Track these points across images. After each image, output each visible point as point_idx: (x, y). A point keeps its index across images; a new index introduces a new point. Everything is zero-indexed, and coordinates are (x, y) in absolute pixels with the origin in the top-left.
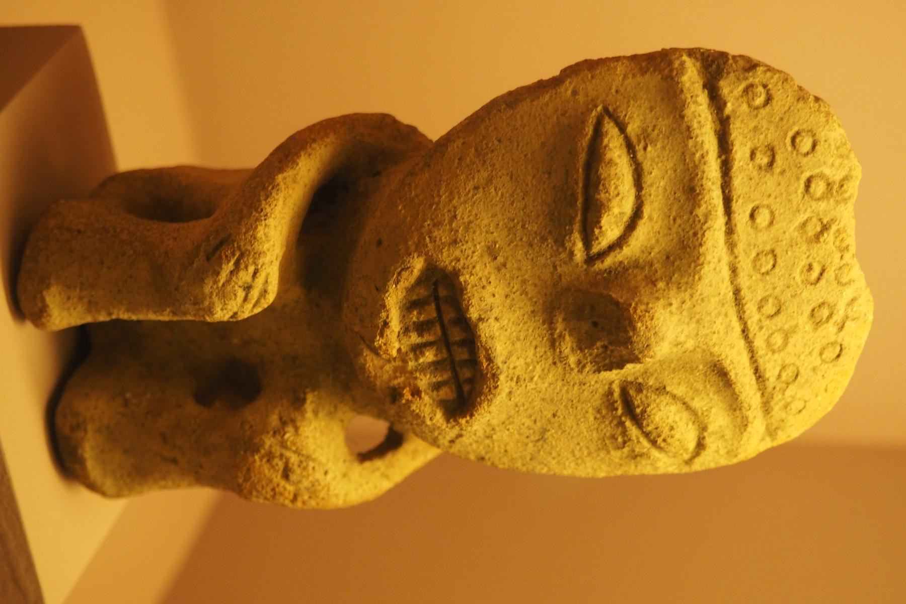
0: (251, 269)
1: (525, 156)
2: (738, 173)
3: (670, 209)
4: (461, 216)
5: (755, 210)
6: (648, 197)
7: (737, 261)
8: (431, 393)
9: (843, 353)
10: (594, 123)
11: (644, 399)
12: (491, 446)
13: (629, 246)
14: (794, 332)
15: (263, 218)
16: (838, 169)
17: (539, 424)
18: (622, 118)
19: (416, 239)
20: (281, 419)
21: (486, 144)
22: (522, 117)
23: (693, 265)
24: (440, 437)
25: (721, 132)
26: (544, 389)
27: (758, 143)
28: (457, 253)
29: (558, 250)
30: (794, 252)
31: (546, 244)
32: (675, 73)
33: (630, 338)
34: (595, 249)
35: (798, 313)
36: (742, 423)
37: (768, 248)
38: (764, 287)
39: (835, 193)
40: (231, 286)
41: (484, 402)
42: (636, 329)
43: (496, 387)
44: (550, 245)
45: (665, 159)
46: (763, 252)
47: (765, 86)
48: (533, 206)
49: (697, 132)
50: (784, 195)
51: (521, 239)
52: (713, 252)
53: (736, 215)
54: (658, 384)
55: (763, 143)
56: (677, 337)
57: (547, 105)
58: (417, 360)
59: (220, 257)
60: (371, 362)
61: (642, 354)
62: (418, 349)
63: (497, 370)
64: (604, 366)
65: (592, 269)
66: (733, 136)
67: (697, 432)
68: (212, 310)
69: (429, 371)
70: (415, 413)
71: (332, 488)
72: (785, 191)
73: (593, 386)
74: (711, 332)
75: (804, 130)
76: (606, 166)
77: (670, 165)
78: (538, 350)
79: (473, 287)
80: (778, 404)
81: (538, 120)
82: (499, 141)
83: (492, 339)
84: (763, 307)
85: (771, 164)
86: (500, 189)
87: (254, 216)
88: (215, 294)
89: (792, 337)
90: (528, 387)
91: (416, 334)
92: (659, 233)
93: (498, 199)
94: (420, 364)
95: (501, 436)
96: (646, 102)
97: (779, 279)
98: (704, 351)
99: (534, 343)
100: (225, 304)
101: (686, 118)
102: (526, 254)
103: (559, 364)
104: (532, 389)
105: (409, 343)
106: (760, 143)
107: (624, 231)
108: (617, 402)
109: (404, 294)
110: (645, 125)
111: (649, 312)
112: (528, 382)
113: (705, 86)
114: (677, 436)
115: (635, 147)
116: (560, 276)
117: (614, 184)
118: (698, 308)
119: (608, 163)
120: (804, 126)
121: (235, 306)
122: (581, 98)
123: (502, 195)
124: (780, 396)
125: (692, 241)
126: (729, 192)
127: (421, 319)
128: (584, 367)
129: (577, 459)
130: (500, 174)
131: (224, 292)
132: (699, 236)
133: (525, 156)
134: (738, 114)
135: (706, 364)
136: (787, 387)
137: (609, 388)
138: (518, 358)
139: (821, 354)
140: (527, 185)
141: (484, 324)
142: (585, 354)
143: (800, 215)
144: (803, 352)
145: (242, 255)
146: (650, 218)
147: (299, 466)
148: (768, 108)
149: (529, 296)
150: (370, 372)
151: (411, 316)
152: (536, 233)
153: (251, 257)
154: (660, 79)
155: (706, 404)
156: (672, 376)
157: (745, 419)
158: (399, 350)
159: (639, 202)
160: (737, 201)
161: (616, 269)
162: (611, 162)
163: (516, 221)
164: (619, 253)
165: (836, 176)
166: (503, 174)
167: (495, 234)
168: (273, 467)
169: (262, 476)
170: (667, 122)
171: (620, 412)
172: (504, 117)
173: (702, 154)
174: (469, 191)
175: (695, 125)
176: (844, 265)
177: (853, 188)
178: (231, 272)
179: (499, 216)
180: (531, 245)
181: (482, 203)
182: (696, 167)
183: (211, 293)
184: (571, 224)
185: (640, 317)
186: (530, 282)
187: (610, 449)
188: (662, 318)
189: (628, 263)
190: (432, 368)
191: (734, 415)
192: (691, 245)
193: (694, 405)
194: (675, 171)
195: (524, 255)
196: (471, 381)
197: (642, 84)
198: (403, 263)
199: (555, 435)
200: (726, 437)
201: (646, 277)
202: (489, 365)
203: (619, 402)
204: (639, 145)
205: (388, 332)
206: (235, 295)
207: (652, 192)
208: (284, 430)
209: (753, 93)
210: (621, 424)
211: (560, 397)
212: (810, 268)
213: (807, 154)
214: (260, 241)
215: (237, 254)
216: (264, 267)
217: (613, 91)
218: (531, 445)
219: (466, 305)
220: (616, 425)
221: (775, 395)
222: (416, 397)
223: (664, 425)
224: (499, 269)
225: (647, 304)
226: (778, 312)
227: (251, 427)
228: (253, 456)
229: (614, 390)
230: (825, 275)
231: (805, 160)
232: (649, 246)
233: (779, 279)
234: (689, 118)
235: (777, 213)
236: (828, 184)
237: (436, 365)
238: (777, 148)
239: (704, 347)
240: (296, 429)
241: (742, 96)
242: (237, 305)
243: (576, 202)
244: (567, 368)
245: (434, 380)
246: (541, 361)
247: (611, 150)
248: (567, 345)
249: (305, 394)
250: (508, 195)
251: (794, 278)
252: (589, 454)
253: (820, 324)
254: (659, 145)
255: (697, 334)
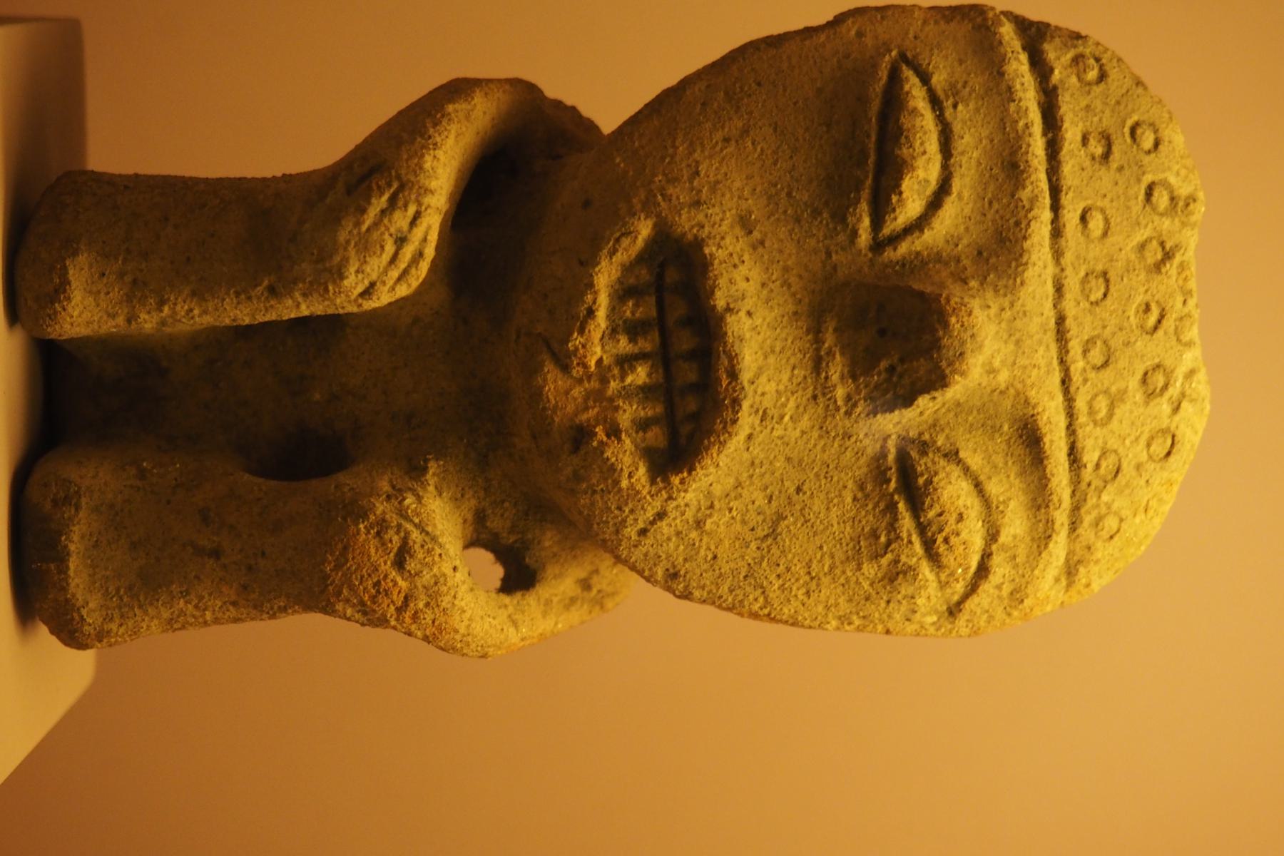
0: (412, 209)
1: (795, 104)
2: (1068, 158)
3: (985, 189)
4: (706, 173)
5: (1087, 212)
6: (958, 168)
7: (1064, 275)
8: (634, 435)
9: (1174, 451)
10: (888, 67)
11: (929, 464)
12: (697, 544)
13: (933, 229)
14: (1122, 400)
15: (431, 146)
16: (1184, 181)
17: (774, 504)
18: (924, 67)
19: (643, 197)
20: (393, 487)
21: (742, 88)
22: (789, 58)
23: (1014, 264)
24: (630, 521)
25: (1046, 105)
26: (793, 440)
27: (1091, 126)
28: (701, 217)
29: (835, 229)
30: (1131, 280)
31: (819, 219)
32: (990, 23)
33: (939, 339)
34: (887, 231)
35: (1128, 371)
36: (1045, 532)
37: (1100, 268)
38: (1093, 323)
39: (1179, 213)
40: (379, 233)
41: (714, 445)
42: (949, 326)
43: (734, 421)
44: (824, 222)
45: (980, 123)
46: (1092, 273)
47: (1098, 60)
48: (805, 169)
49: (1020, 94)
50: (1122, 199)
51: (785, 212)
52: (1039, 251)
53: (1065, 211)
54: (948, 445)
55: (1096, 129)
56: (993, 357)
57: (823, 45)
58: (623, 379)
59: (370, 188)
60: (553, 382)
61: (950, 369)
62: (626, 363)
63: (741, 393)
64: (883, 405)
65: (880, 260)
66: (1062, 111)
67: (984, 542)
68: (343, 271)
69: (636, 399)
70: (609, 463)
71: (459, 595)
72: (1123, 194)
73: (861, 441)
74: (1031, 364)
75: (1144, 121)
76: (910, 115)
77: (985, 133)
78: (796, 372)
79: (721, 263)
80: (1090, 513)
81: (811, 62)
82: (759, 84)
83: (741, 341)
84: (1089, 351)
85: (1106, 156)
86: (759, 143)
87: (420, 143)
88: (353, 244)
89: (1119, 407)
90: (775, 431)
91: (626, 338)
92: (970, 219)
93: (756, 156)
94: (624, 388)
95: (717, 523)
96: (954, 54)
97: (1111, 315)
98: (1018, 394)
99: (792, 361)
100: (365, 262)
101: (1006, 76)
102: (791, 232)
103: (821, 399)
104: (778, 438)
105: (614, 351)
106: (1094, 127)
107: (926, 210)
108: (891, 469)
109: (619, 274)
110: (954, 79)
111: (965, 306)
112: (777, 423)
113: (1024, 49)
114: (964, 535)
115: (942, 102)
116: (835, 268)
117: (920, 138)
118: (1018, 323)
119: (912, 112)
120: (1145, 117)
121: (376, 268)
122: (869, 41)
123: (762, 150)
124: (1094, 500)
125: (1014, 233)
126: (1057, 180)
127: (638, 315)
128: (855, 405)
129: (812, 578)
130: (760, 124)
131: (367, 241)
132: (1023, 226)
133: (795, 104)
134: (1066, 85)
135: (1013, 421)
136: (1105, 487)
137: (882, 447)
138: (769, 381)
139: (1148, 445)
140: (797, 140)
141: (733, 317)
142: (860, 385)
143: (1140, 229)
144: (1129, 435)
145: (402, 187)
146: (960, 197)
147: (422, 546)
148: (1102, 86)
149: (793, 289)
150: (549, 401)
151: (624, 308)
152: (805, 204)
153: (414, 191)
154: (970, 28)
155: (1003, 492)
156: (968, 436)
157: (1050, 524)
158: (600, 361)
159: (947, 173)
160: (1067, 194)
161: (912, 262)
162: (914, 111)
163: (779, 186)
164: (918, 238)
165: (1183, 191)
166: (765, 125)
167: (750, 201)
168: (383, 544)
169: (365, 559)
170: (980, 79)
171: (893, 485)
172: (765, 57)
173: (1027, 124)
174: (717, 143)
175: (1018, 87)
176: (1185, 316)
177: (1199, 209)
178: (383, 212)
179: (757, 179)
180: (798, 220)
181: (733, 160)
182: (1019, 138)
183: (348, 242)
184: (858, 190)
185: (954, 309)
186: (794, 272)
187: (864, 560)
188: (980, 319)
189: (929, 255)
190: (641, 396)
191: (1036, 517)
192: (1011, 237)
193: (989, 489)
194: (992, 141)
195: (787, 233)
196: (695, 417)
197: (947, 33)
198: (625, 224)
199: (792, 528)
200: (1017, 559)
201: (952, 274)
202: (730, 383)
203: (893, 470)
204: (947, 101)
205: (591, 326)
206: (382, 247)
207: (964, 162)
208: (402, 495)
209: (1084, 64)
210: (892, 507)
211: (813, 457)
212: (1147, 309)
213: (1149, 152)
214: (427, 174)
215: (395, 185)
216: (429, 211)
217: (911, 35)
218: (753, 546)
219: (710, 287)
220: (883, 510)
221: (1089, 496)
222: (613, 438)
223: (952, 509)
224: (754, 248)
225: (962, 298)
226: (1106, 364)
227: (352, 489)
228: (357, 524)
229: (889, 450)
230: (1164, 322)
231: (1146, 159)
232: (956, 234)
233: (1111, 315)
234: (1011, 76)
235: (1112, 220)
236: (1172, 199)
237: (646, 392)
238: (1113, 137)
239: (1019, 386)
240: (419, 499)
241: (1071, 66)
242: (379, 267)
243: (867, 160)
244: (831, 407)
245: (642, 414)
246: (796, 392)
247: (914, 98)
248: (836, 369)
249: (426, 461)
250: (769, 152)
251: (1129, 318)
252: (831, 568)
253: (1151, 397)
254: (972, 106)
255: (1014, 363)
